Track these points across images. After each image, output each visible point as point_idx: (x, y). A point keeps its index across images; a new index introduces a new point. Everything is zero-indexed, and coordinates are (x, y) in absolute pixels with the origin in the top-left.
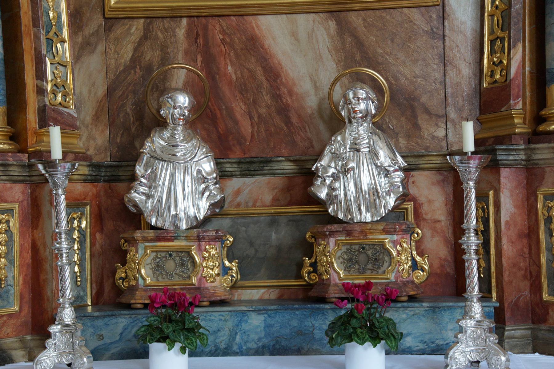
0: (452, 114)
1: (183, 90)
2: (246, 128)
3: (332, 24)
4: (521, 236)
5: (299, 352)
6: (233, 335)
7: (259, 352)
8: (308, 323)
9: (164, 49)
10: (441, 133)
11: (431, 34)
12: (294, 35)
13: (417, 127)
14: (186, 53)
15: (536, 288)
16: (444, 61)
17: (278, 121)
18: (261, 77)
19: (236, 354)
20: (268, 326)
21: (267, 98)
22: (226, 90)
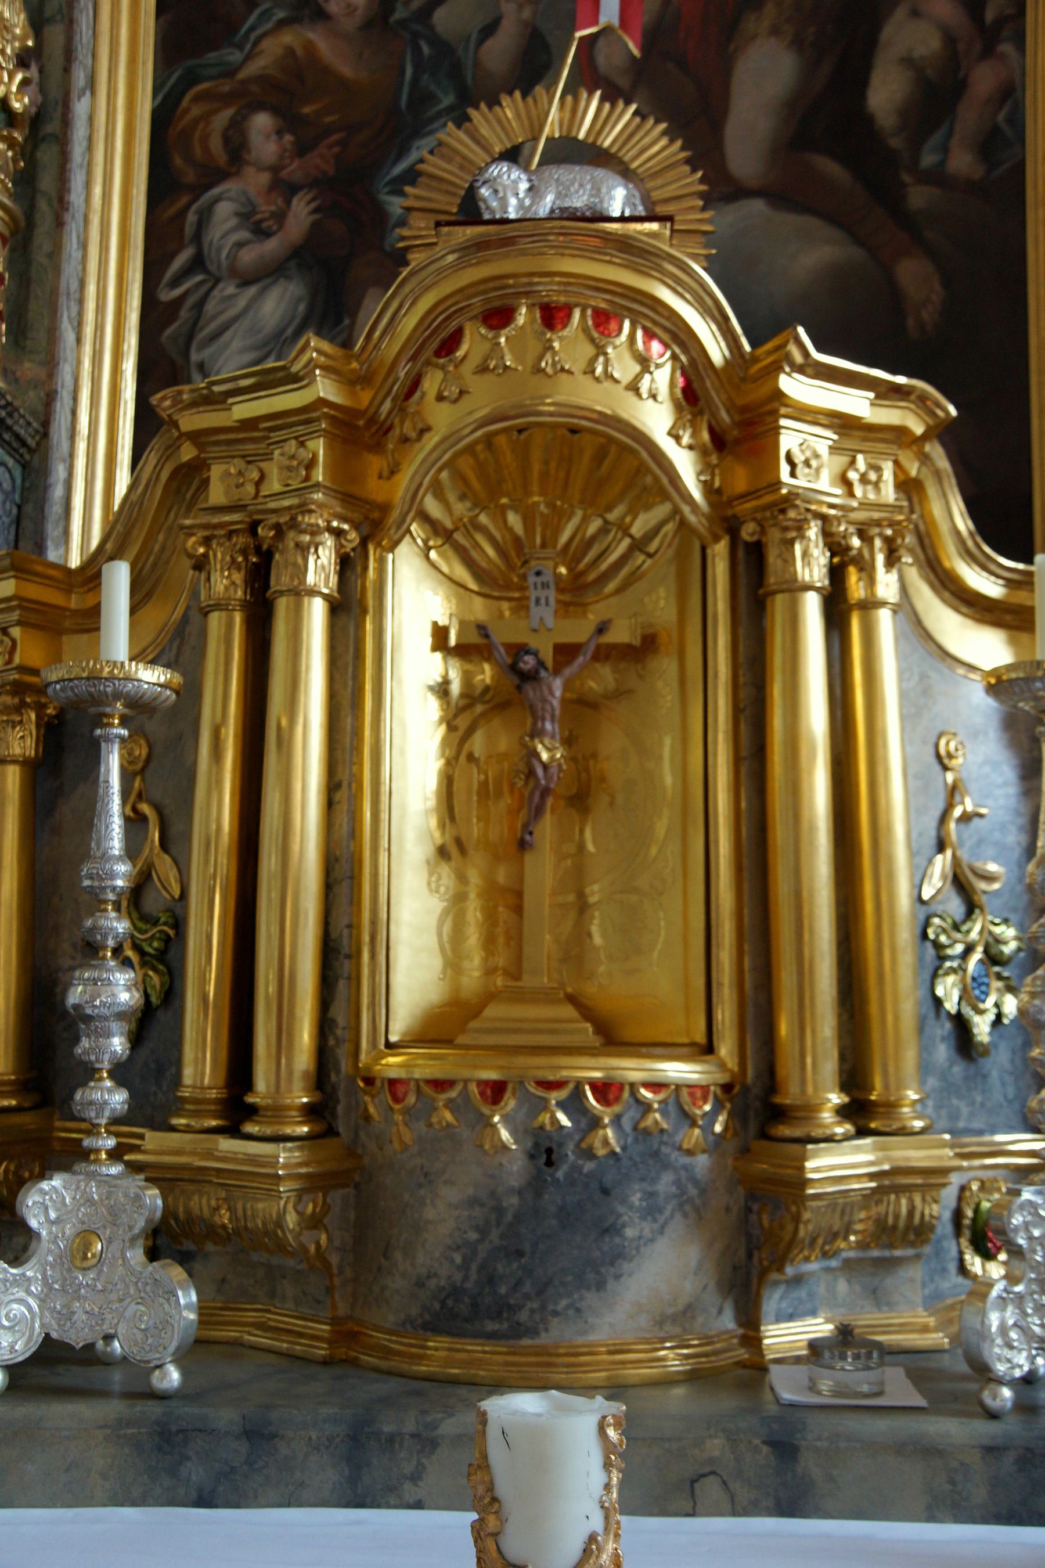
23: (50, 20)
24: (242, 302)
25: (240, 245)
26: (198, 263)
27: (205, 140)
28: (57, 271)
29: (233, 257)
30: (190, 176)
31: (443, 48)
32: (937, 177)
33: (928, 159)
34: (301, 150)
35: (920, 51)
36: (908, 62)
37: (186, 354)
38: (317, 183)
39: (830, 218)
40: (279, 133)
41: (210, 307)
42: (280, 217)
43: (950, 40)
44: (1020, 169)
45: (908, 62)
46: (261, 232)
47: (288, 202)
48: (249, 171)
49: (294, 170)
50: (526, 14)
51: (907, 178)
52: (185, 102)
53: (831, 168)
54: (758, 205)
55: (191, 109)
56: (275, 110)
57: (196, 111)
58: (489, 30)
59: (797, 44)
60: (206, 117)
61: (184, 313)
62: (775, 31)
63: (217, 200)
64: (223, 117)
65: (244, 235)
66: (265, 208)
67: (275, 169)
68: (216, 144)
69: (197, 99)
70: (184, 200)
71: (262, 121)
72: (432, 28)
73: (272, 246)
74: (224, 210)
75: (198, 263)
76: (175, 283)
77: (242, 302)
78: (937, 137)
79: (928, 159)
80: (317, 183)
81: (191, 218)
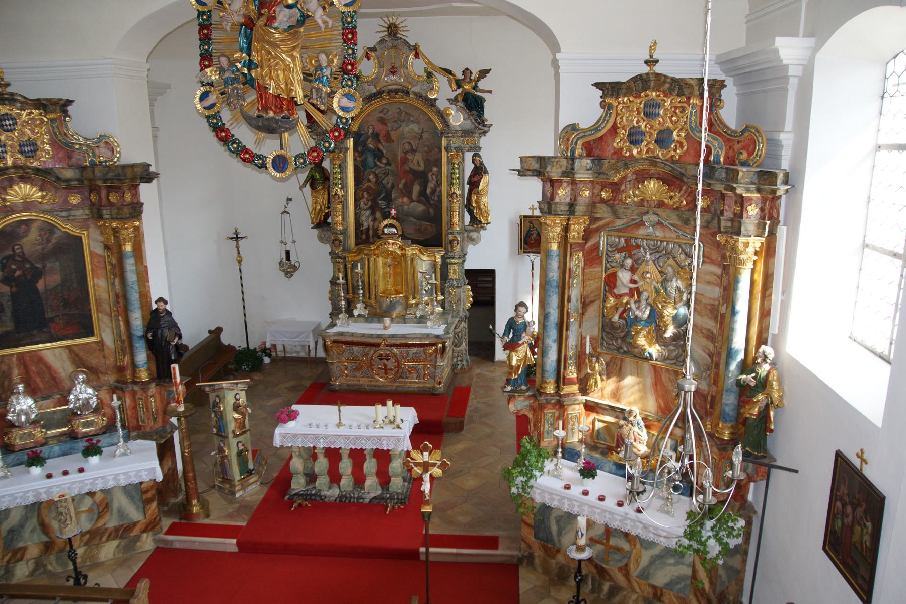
0: (109, 373)
1: (20, 383)
2: (41, 385)
3: (67, 351)
4: (133, 408)
5: (71, 454)
6: (50, 453)
7: (58, 456)
8: (73, 445)
9: (8, 365)
10: (106, 378)
11: (100, 350)
12: (55, 355)
13: (99, 378)
14: (17, 365)
15: (138, 421)
16: (104, 357)
17: (52, 382)
18: (44, 369)
19: (53, 458)
20: (60, 449)
21: (48, 376)
22: (33, 376)
32: (434, 200)
53: (423, 199)
55: (358, 192)
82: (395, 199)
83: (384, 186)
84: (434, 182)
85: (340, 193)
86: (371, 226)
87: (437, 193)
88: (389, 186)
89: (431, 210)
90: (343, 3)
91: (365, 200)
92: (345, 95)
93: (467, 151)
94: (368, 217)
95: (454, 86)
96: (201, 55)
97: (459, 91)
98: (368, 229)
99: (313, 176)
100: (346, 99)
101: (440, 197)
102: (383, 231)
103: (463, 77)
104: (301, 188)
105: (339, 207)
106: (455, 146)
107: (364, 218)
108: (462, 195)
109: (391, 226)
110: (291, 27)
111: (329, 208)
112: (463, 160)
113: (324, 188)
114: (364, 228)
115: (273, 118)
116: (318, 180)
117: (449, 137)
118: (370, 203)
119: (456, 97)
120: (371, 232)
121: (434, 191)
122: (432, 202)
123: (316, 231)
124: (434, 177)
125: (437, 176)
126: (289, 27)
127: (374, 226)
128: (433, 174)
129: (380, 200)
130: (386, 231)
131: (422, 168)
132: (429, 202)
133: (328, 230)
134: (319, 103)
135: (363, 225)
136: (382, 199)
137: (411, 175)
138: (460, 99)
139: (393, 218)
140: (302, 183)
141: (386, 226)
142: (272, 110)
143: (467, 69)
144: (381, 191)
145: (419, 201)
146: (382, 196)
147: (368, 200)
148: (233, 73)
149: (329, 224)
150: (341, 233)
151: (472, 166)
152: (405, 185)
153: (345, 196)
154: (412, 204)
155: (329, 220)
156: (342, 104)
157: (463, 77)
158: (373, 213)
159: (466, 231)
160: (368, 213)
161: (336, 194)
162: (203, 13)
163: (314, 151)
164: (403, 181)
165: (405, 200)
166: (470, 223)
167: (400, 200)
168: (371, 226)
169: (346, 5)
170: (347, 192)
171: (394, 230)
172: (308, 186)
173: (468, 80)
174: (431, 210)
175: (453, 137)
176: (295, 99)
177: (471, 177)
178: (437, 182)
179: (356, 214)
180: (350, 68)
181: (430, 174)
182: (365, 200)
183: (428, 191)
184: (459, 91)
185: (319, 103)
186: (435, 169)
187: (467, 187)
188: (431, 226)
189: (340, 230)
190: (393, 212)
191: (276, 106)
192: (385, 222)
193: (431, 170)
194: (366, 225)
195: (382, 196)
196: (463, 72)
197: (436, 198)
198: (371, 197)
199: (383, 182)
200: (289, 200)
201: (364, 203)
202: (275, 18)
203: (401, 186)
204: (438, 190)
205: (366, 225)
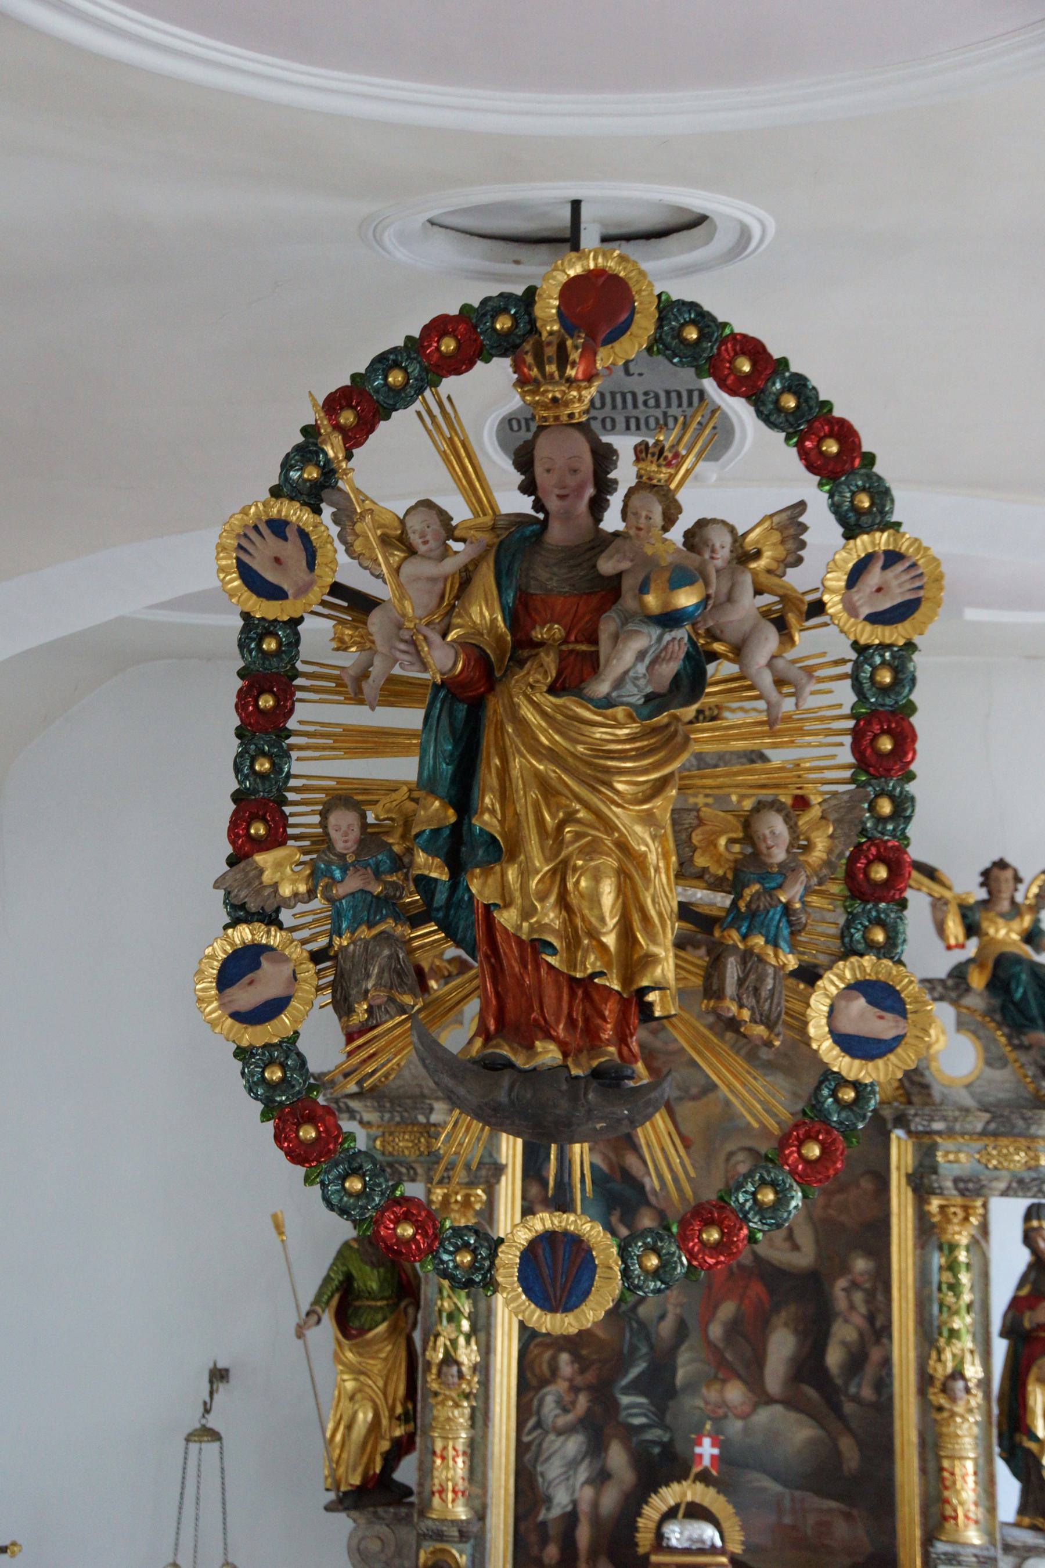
23: (480, 1330)
24: (558, 1444)
25: (556, 1416)
26: (539, 1425)
27: (540, 1366)
28: (486, 1446)
29: (554, 1422)
30: (534, 1382)
31: (642, 1325)
32: (856, 1399)
33: (853, 1390)
34: (582, 1371)
35: (848, 1339)
36: (844, 1343)
37: (535, 1467)
38: (590, 1388)
39: (811, 1416)
40: (572, 1362)
41: (545, 1445)
42: (573, 1403)
43: (861, 1335)
44: (891, 1398)
45: (844, 1343)
46: (566, 1410)
47: (577, 1396)
48: (560, 1381)
49: (579, 1381)
50: (678, 1311)
51: (843, 1398)
52: (532, 1347)
53: (811, 1392)
54: (778, 1409)
56: (570, 1352)
57: (536, 1352)
58: (662, 1317)
59: (796, 1331)
60: (540, 1355)
61: (534, 1448)
62: (786, 1325)
63: (546, 1395)
64: (547, 1355)
65: (558, 1411)
66: (567, 1399)
67: (571, 1380)
68: (545, 1367)
69: (536, 1346)
70: (532, 1394)
71: (564, 1357)
72: (637, 1315)
73: (570, 1418)
74: (550, 1402)
75: (539, 1425)
76: (530, 1433)
77: (558, 1444)
78: (856, 1380)
79: (853, 1390)
80: (590, 1388)
81: (535, 1403)
82: (692, 1387)
83: (644, 1330)
84: (858, 1320)
85: (468, 1355)
86: (584, 1507)
87: (870, 1371)
88: (666, 1329)
89: (847, 1445)
90: (865, 611)
91: (560, 1386)
92: (862, 987)
93: (1004, 1193)
94: (573, 1465)
95: (954, 928)
96: (237, 797)
97: (972, 947)
98: (571, 1518)
99: (349, 1278)
100: (862, 1002)
101: (883, 1384)
102: (659, 1536)
103: (982, 894)
104: (300, 1334)
105: (461, 1416)
106: (956, 1170)
107: (552, 1469)
108: (985, 1383)
109: (696, 1512)
110: (655, 702)
111: (408, 1417)
112: (984, 1229)
113: (393, 1330)
114: (556, 1512)
115: (552, 1071)
116: (371, 1295)
117: (930, 1133)
118: (583, 1402)
119: (959, 973)
120: (583, 1535)
121: (856, 1362)
122: (849, 1408)
123: (343, 1523)
124: (858, 1297)
125: (870, 1297)
126: (649, 698)
127: (595, 1505)
128: (855, 1285)
129: (626, 1391)
130: (676, 1534)
131: (804, 1258)
132: (836, 1408)
133: (399, 1520)
134: (746, 1014)
135: (548, 1500)
136: (634, 1388)
137: (757, 1290)
138: (978, 980)
139: (704, 1477)
140: (305, 1307)
141: (671, 1514)
142: (549, 1036)
143: (1001, 864)
144: (634, 1349)
145: (790, 1403)
146: (634, 1372)
147: (575, 1389)
148: (377, 874)
149: (408, 1491)
150: (463, 1536)
151: (1023, 1257)
152: (733, 1329)
153: (484, 1369)
154: (764, 1415)
155: (406, 1472)
156: (847, 1027)
157: (982, 894)
158: (596, 1448)
159: (1008, 1548)
160: (574, 1444)
161: (450, 1360)
162: (268, 628)
163: (709, 1223)
164: (727, 1310)
165: (735, 1393)
166: (1022, 1510)
167: (712, 1394)
168: (584, 1507)
169: (874, 619)
170: (487, 1351)
171: (709, 1534)
172: (328, 1320)
173: (1005, 906)
174: (847, 1445)
175: (950, 1133)
176: (652, 997)
177: (1016, 1304)
178: (871, 1318)
179: (521, 1448)
180: (881, 873)
181: (842, 1283)
182: (560, 1386)
183: (834, 1358)
184: (972, 947)
185: (746, 1014)
186: (861, 1265)
187: (1000, 1347)
188: (848, 1517)
189: (455, 1522)
190: (707, 1450)
191: (571, 1022)
192: (670, 1495)
193: (845, 1269)
194: (561, 1499)
195: (634, 1372)
196: (986, 874)
197: (867, 1393)
198: (590, 1376)
199: (642, 1310)
200: (219, 1375)
201: (559, 1402)
202: (592, 665)
203: (716, 1331)
204: (875, 1355)
205: (561, 1499)
